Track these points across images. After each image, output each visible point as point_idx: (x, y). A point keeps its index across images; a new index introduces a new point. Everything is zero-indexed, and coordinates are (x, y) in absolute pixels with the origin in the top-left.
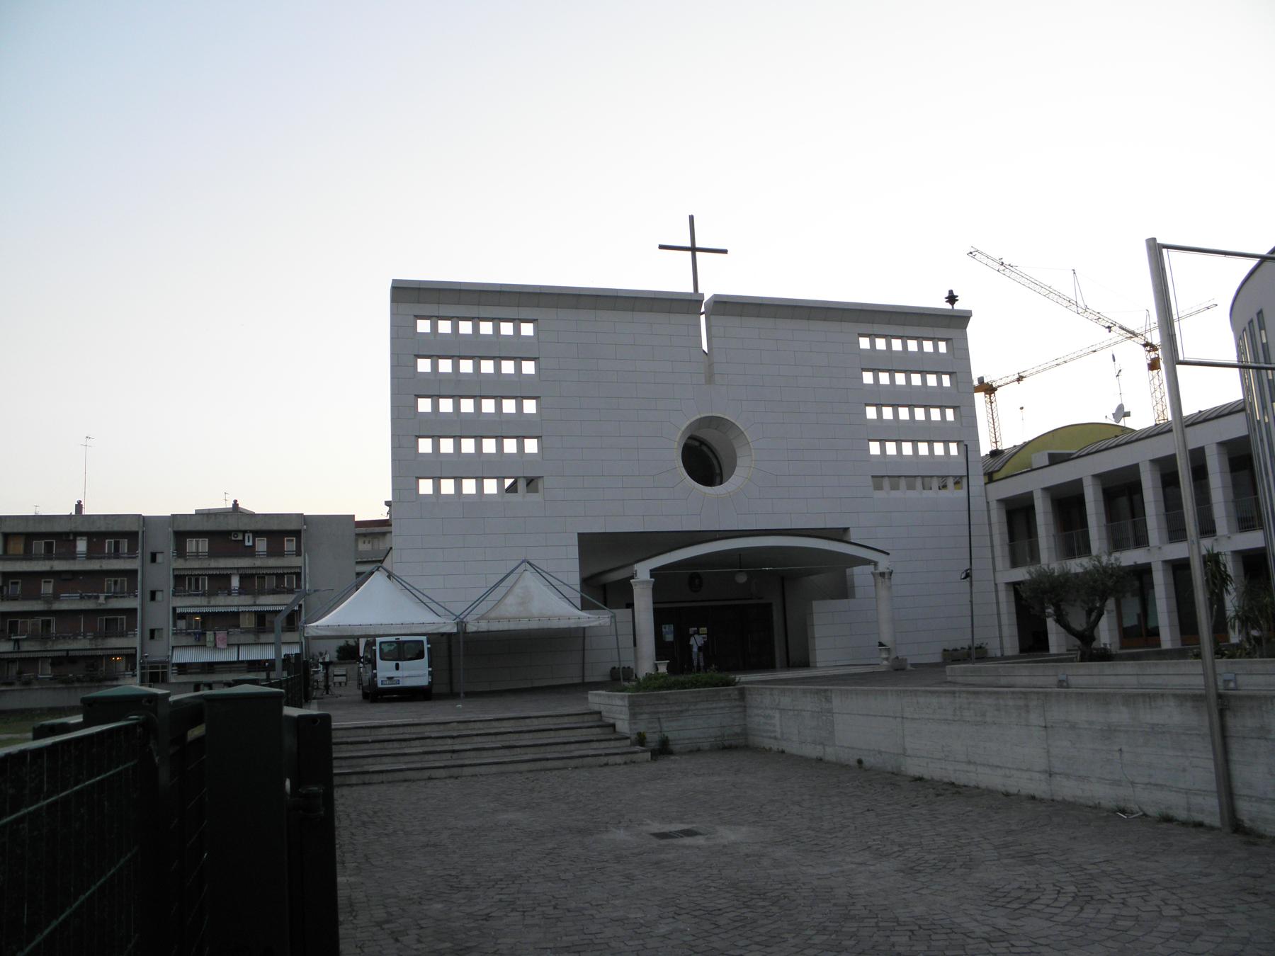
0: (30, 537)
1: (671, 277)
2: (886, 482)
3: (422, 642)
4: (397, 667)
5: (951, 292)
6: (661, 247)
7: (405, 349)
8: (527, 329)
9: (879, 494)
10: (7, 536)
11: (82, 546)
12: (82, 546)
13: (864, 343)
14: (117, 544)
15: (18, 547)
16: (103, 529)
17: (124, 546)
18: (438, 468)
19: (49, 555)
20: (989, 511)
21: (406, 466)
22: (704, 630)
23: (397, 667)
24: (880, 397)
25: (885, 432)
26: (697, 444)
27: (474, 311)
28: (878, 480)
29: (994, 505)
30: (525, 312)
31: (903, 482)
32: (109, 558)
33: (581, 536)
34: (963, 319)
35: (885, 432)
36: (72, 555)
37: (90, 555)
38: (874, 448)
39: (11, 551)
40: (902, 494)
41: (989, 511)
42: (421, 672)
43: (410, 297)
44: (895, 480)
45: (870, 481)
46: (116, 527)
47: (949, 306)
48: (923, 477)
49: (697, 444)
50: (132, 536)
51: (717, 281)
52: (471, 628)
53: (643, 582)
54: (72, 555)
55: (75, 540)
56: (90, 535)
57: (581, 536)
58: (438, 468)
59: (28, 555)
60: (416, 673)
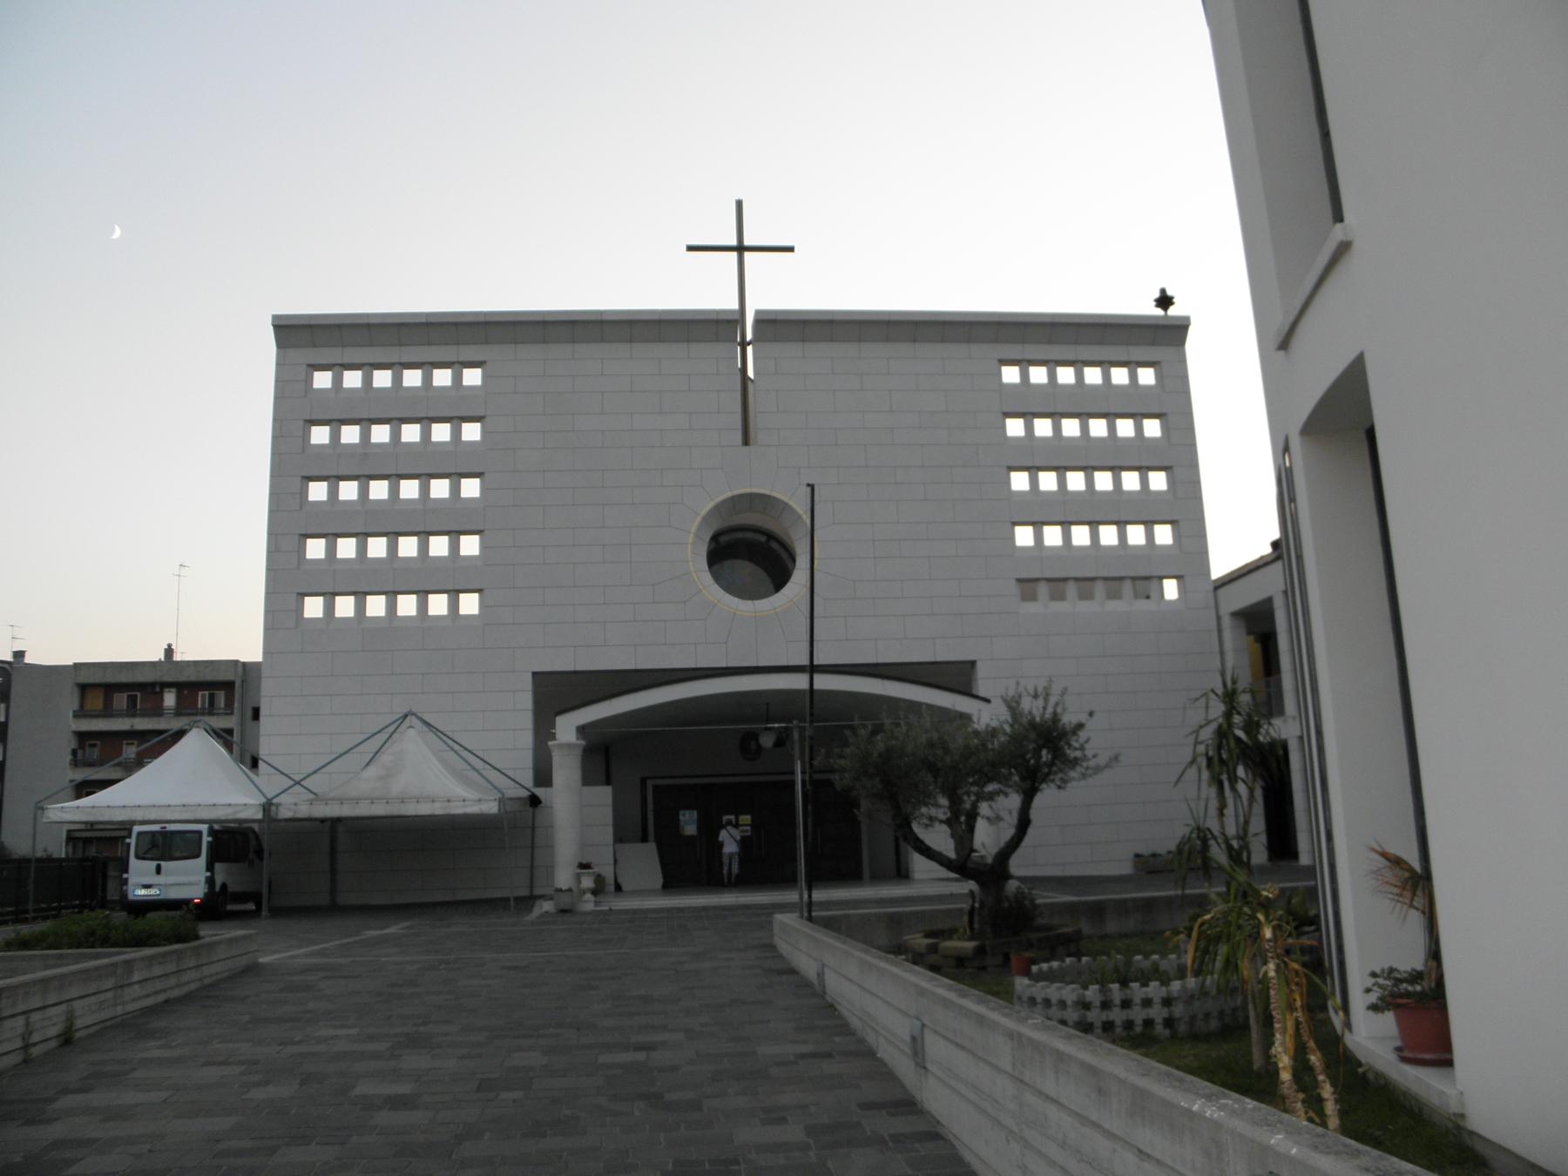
0: (110, 689)
1: (705, 289)
2: (1043, 589)
3: (200, 833)
4: (159, 870)
5: (1163, 291)
6: (691, 248)
7: (294, 411)
8: (472, 377)
9: (1031, 608)
10: (84, 688)
11: (170, 699)
12: (170, 699)
13: (1010, 375)
14: (212, 697)
15: (96, 701)
16: (193, 678)
17: (221, 697)
18: (335, 580)
19: (132, 711)
20: (1220, 631)
21: (287, 579)
22: (746, 819)
23: (159, 870)
24: (1034, 458)
25: (1040, 511)
26: (763, 539)
27: (394, 354)
28: (1027, 586)
29: (1227, 622)
30: (468, 353)
31: (1099, 588)
32: (203, 714)
33: (534, 674)
34: (1177, 331)
35: (1040, 511)
36: (158, 711)
37: (179, 711)
38: (1024, 536)
39: (88, 707)
40: (1071, 606)
41: (1220, 631)
42: (192, 879)
43: (301, 337)
44: (1086, 583)
45: (1014, 588)
46: (208, 676)
47: (1160, 312)
48: (1134, 579)
49: (763, 539)
50: (228, 686)
51: (777, 289)
52: (285, 813)
53: (569, 746)
54: (158, 711)
55: (162, 693)
56: (179, 687)
57: (534, 674)
58: (335, 580)
59: (108, 712)
60: (186, 879)
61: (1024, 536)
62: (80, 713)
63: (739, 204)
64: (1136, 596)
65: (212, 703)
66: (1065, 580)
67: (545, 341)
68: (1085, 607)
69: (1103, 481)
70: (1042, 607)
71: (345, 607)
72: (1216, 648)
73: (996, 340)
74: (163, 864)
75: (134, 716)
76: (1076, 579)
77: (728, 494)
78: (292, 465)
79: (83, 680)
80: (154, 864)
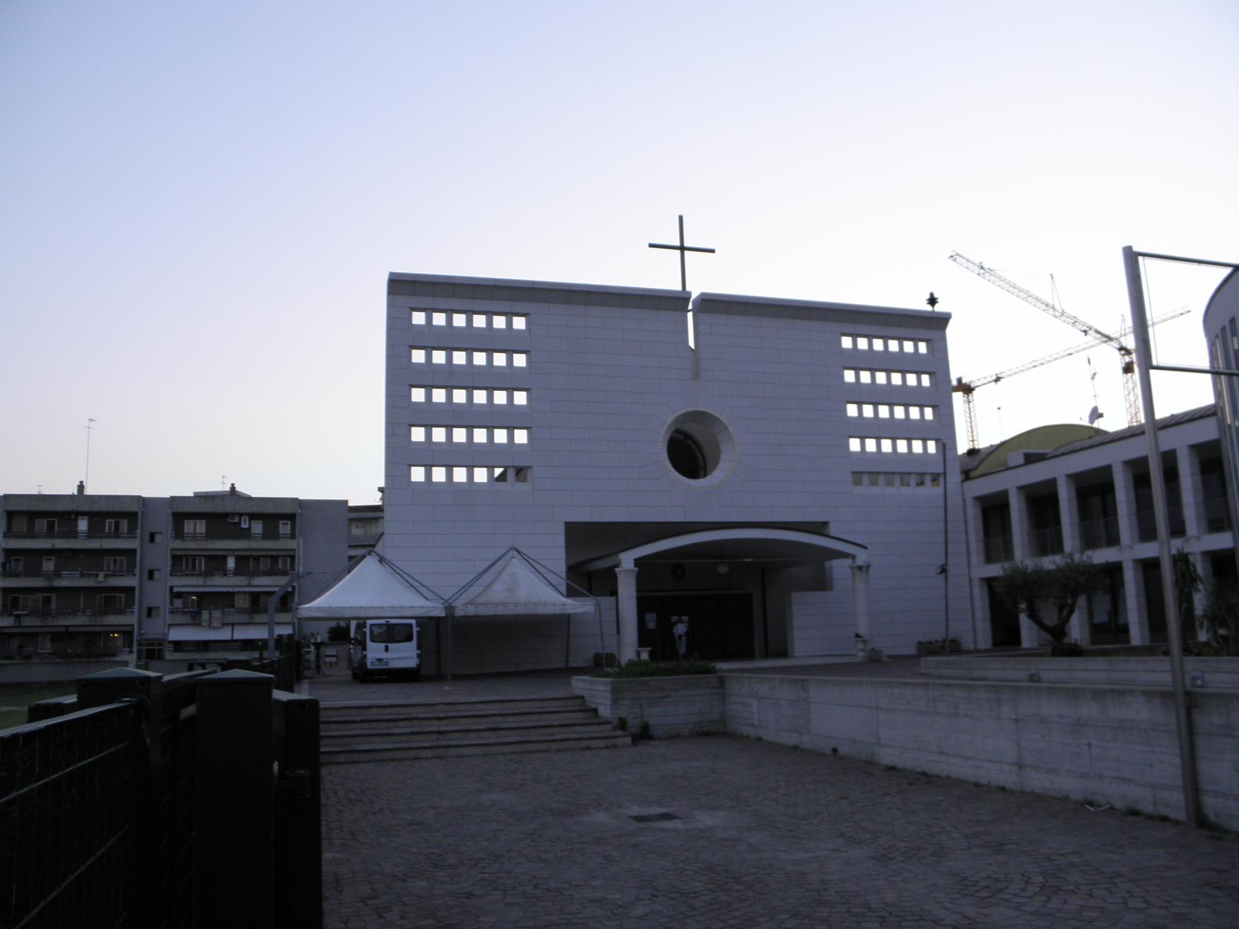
0: (32, 515)
1: (659, 275)
2: (866, 478)
3: (410, 625)
4: (387, 649)
5: (932, 294)
6: (651, 246)
7: (400, 338)
8: (519, 323)
9: (858, 489)
10: (10, 515)
11: (83, 525)
12: (83, 525)
13: (847, 342)
14: (117, 524)
15: (21, 525)
16: (104, 509)
17: (124, 525)
18: (430, 455)
19: (51, 534)
20: (965, 507)
21: (399, 455)
22: (685, 618)
23: (387, 649)
25: (865, 429)
26: (682, 437)
27: (468, 304)
28: (857, 476)
29: (970, 502)
30: (517, 307)
31: (882, 479)
32: (110, 537)
33: (566, 523)
34: (942, 321)
35: (865, 429)
36: (73, 534)
37: (91, 534)
38: (855, 445)
39: (14, 529)
40: (881, 490)
41: (965, 507)
42: (409, 655)
43: (406, 289)
44: (874, 476)
45: (849, 477)
46: (117, 508)
47: (929, 308)
48: (901, 474)
49: (682, 437)
50: (131, 516)
51: (706, 279)
52: (459, 612)
53: (627, 571)
54: (73, 534)
55: (76, 521)
56: (91, 515)
57: (566, 523)
58: (430, 455)
59: (31, 534)
60: (404, 655)
61: (855, 445)
62: (9, 534)
63: (681, 218)
64: (902, 484)
65: (117, 529)
66: (878, 473)
67: (622, 306)
68: (889, 490)
69: (899, 412)
70: (865, 490)
71: (460, 475)
72: (942, 518)
73: (840, 321)
74: (390, 645)
75: (53, 537)
76: (885, 473)
77: (683, 411)
78: (400, 378)
79: (11, 508)
80: (383, 645)
